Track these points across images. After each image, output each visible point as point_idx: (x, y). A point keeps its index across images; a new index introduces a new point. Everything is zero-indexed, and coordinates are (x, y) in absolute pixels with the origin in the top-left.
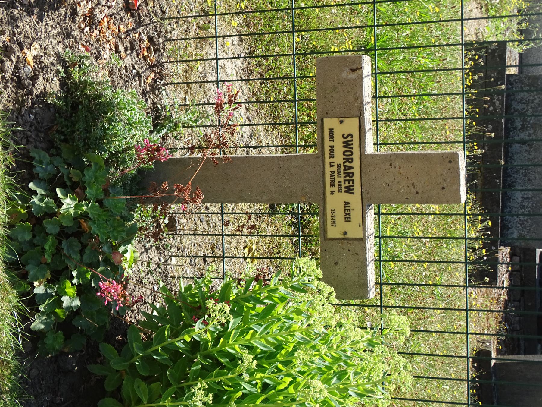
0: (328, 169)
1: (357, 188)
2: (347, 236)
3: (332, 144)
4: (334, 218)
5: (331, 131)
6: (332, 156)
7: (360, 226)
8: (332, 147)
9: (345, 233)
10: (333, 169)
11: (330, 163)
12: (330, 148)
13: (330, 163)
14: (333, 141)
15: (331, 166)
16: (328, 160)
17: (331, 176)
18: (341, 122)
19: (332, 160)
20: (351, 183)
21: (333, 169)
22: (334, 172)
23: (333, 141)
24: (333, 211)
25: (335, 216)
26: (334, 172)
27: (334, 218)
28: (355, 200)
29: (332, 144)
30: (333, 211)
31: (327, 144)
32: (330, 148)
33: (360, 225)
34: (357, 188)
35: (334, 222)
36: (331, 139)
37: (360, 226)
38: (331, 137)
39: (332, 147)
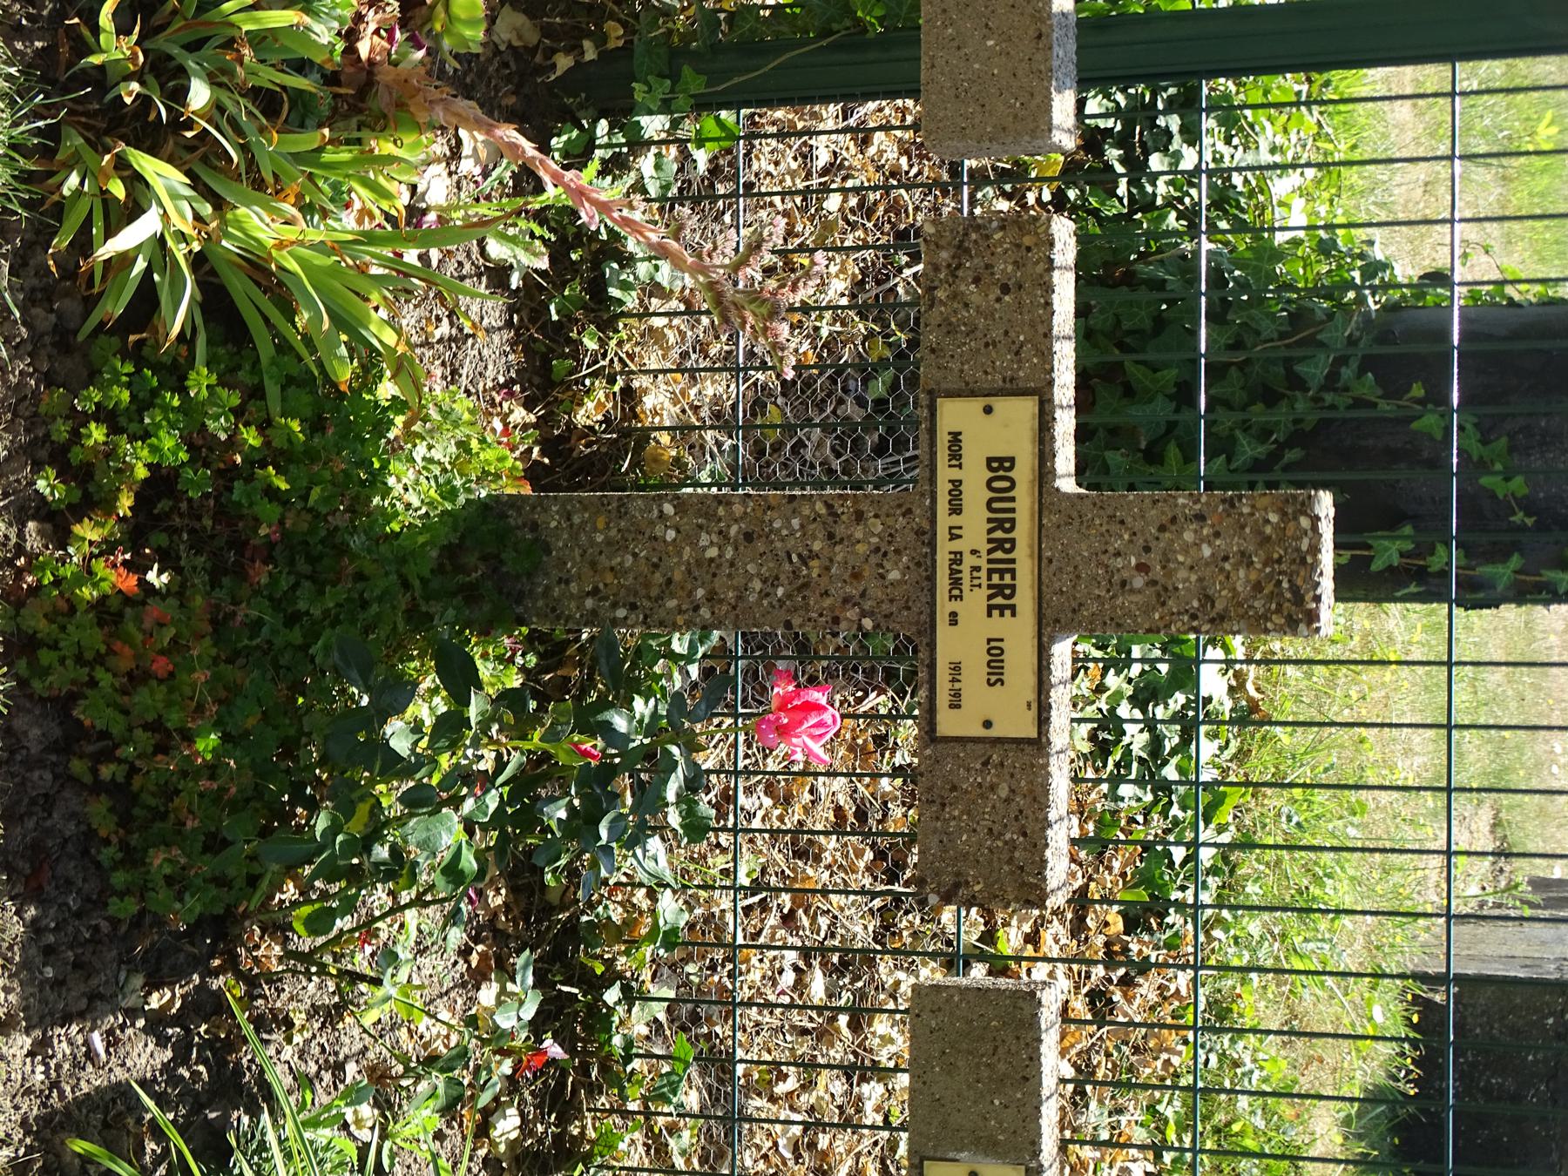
0: (944, 548)
1: (1025, 599)
2: (994, 733)
3: (955, 474)
4: (957, 686)
5: (956, 438)
6: (956, 510)
8: (956, 484)
9: (988, 724)
10: (956, 545)
11: (951, 528)
12: (950, 486)
13: (951, 528)
14: (960, 466)
16: (944, 520)
17: (953, 562)
18: (988, 410)
19: (956, 520)
20: (1008, 577)
21: (956, 545)
23: (960, 466)
27: (957, 686)
28: (1019, 632)
29: (955, 474)
30: (956, 668)
31: (945, 474)
32: (950, 486)
33: (1029, 705)
34: (1025, 599)
35: (957, 694)
38: (955, 456)
39: (956, 484)
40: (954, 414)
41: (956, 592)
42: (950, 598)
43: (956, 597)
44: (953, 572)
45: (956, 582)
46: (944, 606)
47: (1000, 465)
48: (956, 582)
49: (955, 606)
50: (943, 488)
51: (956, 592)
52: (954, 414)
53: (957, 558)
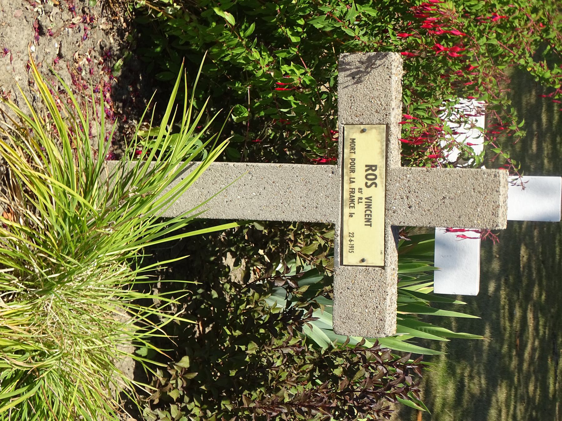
3: (353, 156)
5: (353, 141)
6: (353, 171)
10: (353, 186)
11: (350, 178)
12: (350, 161)
13: (350, 178)
14: (355, 153)
19: (353, 175)
21: (353, 186)
22: (354, 189)
24: (352, 235)
26: (354, 189)
27: (352, 243)
30: (352, 235)
32: (350, 161)
35: (352, 247)
38: (353, 148)
40: (352, 133)
41: (352, 205)
42: (350, 207)
43: (352, 207)
44: (351, 196)
45: (352, 201)
46: (347, 211)
49: (352, 211)
50: (347, 162)
51: (352, 205)
53: (352, 191)
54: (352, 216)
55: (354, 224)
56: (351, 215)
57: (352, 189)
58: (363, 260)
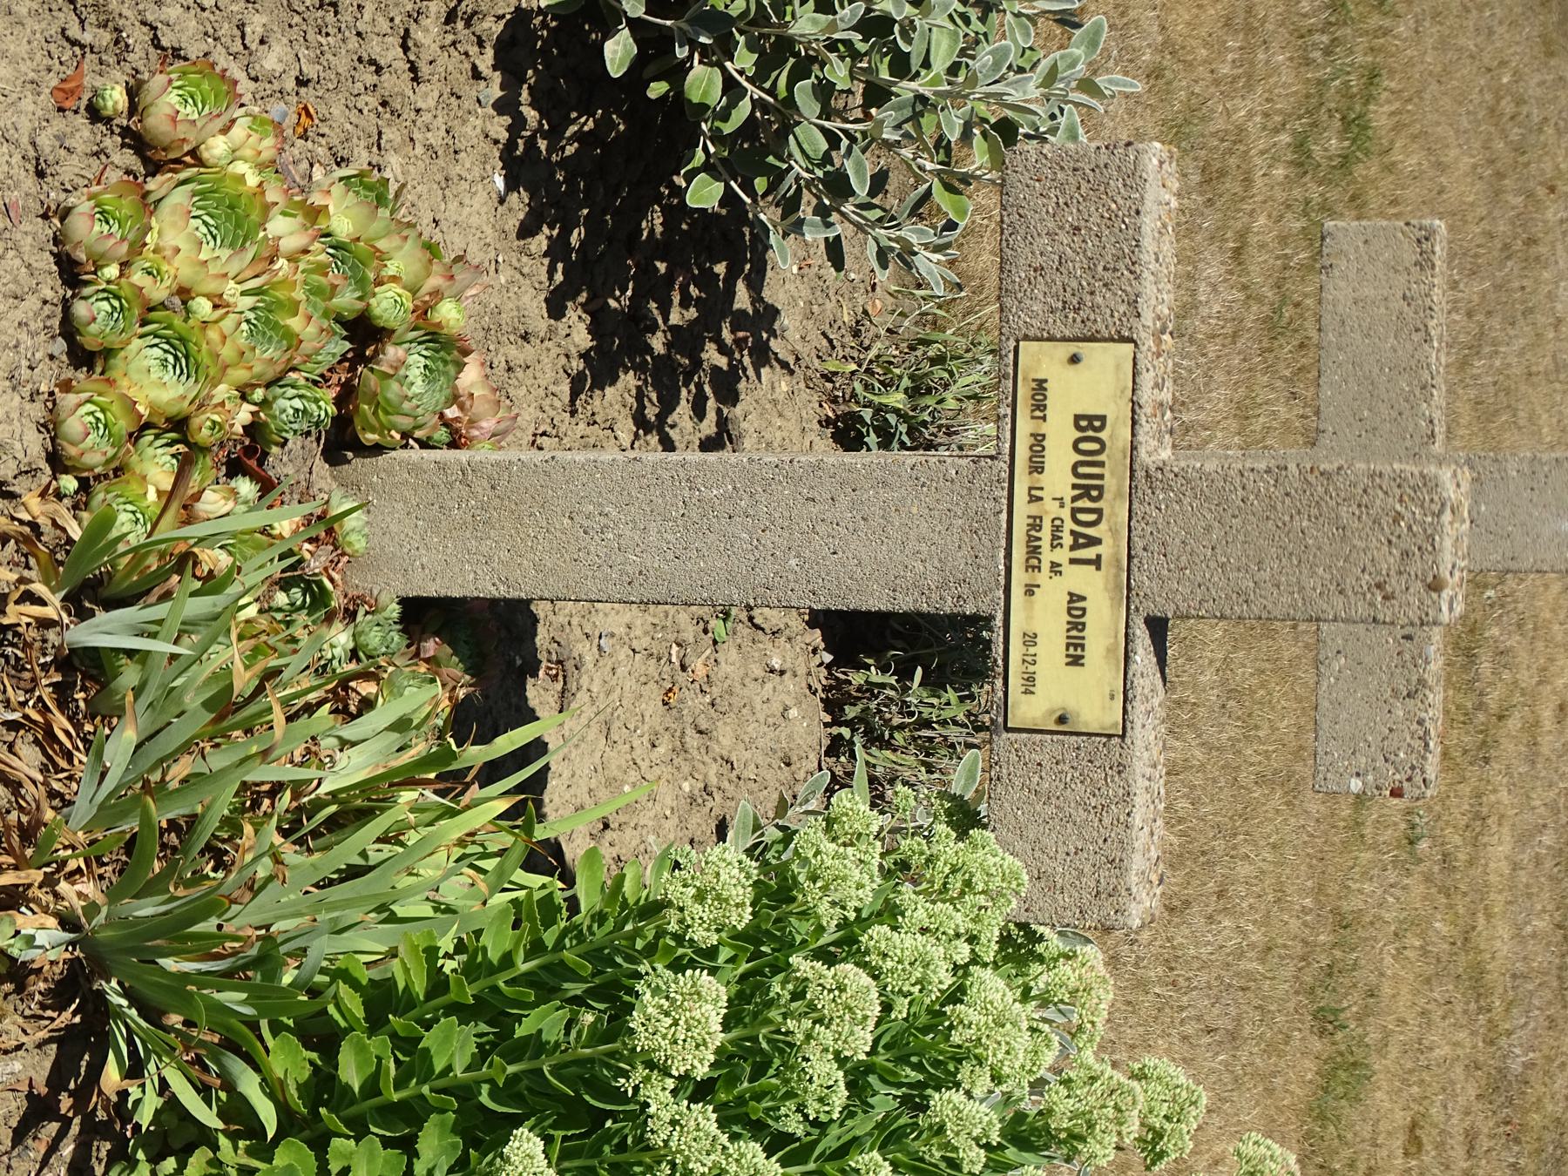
4: (1031, 669)
5: (1041, 385)
6: (1037, 467)
7: (1112, 697)
8: (1039, 439)
10: (1034, 509)
13: (1030, 489)
14: (1044, 418)
15: (1034, 499)
18: (1075, 359)
25: (1035, 663)
27: (1031, 669)
31: (1025, 426)
32: (1032, 440)
35: (1030, 680)
36: (1038, 413)
37: (1112, 697)
38: (1039, 406)
43: (1033, 568)
45: (1033, 551)
46: (1019, 577)
47: (1089, 424)
48: (1033, 551)
51: (1035, 562)
52: (1041, 360)
54: (1033, 593)
55: (1037, 617)
56: (1030, 590)
57: (1034, 518)
58: (1062, 720)
